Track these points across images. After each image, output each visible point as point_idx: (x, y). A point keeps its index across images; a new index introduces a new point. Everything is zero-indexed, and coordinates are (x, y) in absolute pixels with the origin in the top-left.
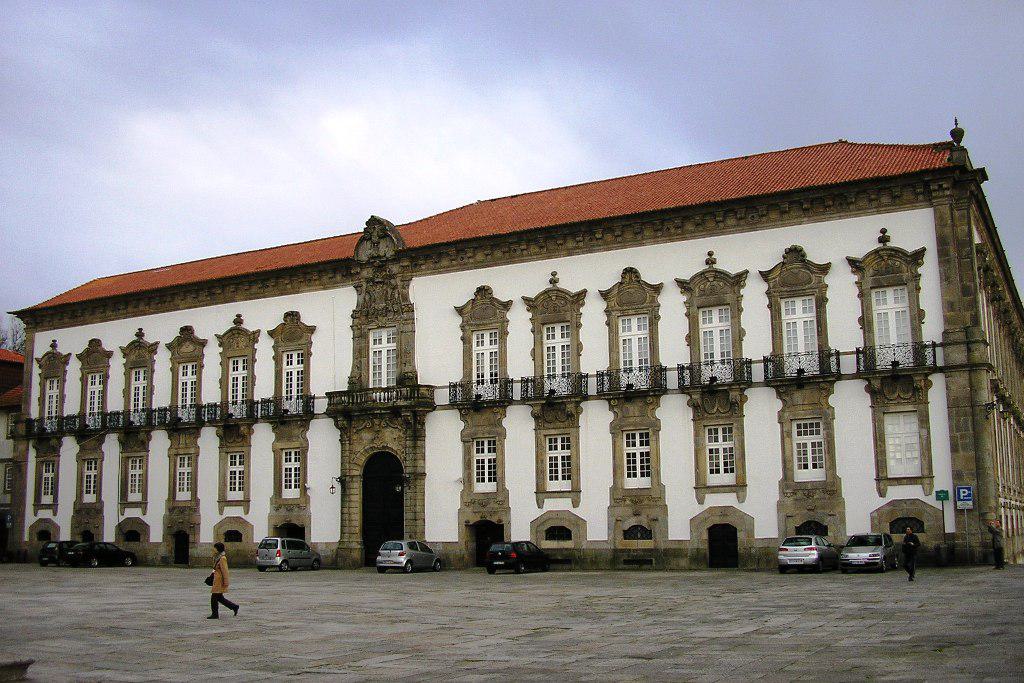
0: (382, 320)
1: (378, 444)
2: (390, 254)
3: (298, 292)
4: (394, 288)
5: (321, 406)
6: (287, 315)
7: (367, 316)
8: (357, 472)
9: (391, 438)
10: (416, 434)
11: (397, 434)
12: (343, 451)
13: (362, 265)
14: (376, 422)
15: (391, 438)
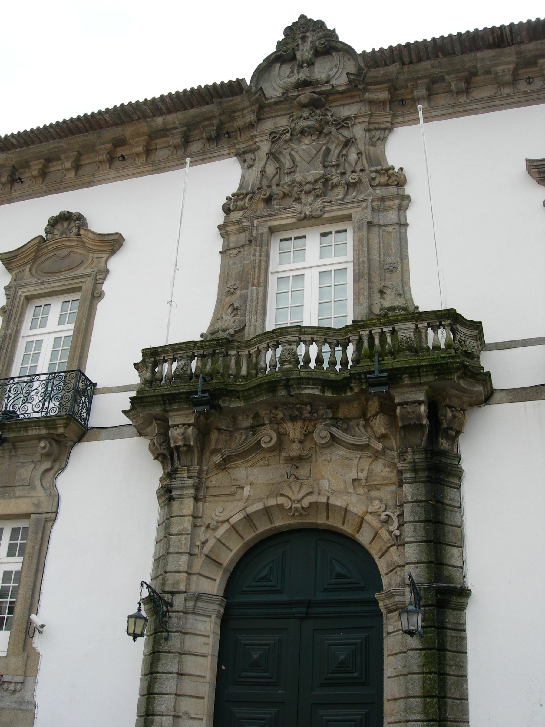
0: (309, 205)
1: (296, 496)
2: (341, 81)
3: (89, 184)
4: (348, 143)
5: (110, 410)
6: (54, 222)
7: (268, 200)
8: (213, 585)
9: (352, 484)
10: (437, 474)
11: (359, 467)
12: (166, 525)
13: (263, 109)
14: (294, 430)
15: (352, 484)
